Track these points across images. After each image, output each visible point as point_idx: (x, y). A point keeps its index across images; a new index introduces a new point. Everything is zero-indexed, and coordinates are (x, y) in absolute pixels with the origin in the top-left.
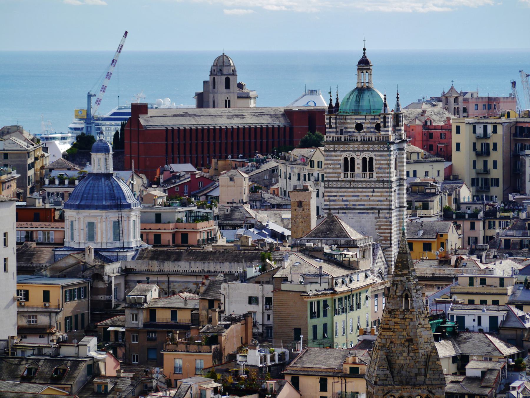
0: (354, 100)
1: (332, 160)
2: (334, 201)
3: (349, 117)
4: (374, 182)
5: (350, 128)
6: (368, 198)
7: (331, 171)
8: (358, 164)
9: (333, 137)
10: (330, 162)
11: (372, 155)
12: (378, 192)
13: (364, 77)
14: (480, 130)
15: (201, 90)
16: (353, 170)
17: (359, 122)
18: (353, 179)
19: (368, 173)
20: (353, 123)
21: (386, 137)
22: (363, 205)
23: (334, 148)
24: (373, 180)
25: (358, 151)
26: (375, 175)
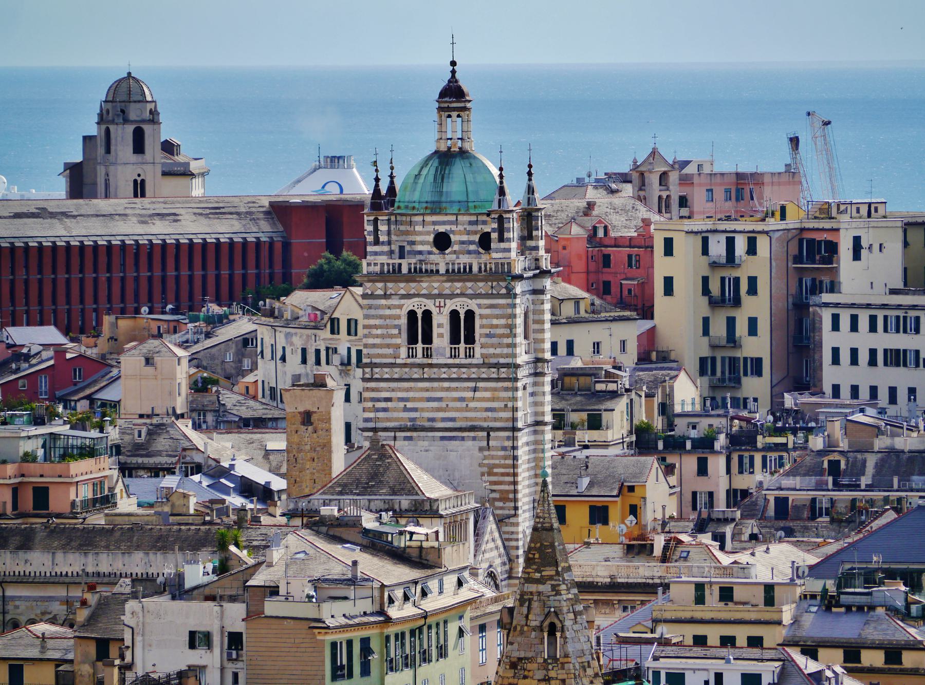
0: (431, 178)
1: (381, 317)
2: (385, 410)
3: (420, 218)
4: (477, 366)
5: (422, 243)
6: (464, 405)
7: (377, 341)
8: (439, 326)
9: (382, 264)
10: (377, 322)
11: (473, 305)
12: (486, 389)
13: (454, 127)
14: (718, 248)
15: (79, 158)
16: (428, 339)
17: (442, 229)
18: (430, 361)
19: (462, 345)
20: (428, 233)
21: (503, 264)
22: (452, 420)
23: (386, 289)
24: (474, 361)
25: (440, 296)
26: (478, 351)
